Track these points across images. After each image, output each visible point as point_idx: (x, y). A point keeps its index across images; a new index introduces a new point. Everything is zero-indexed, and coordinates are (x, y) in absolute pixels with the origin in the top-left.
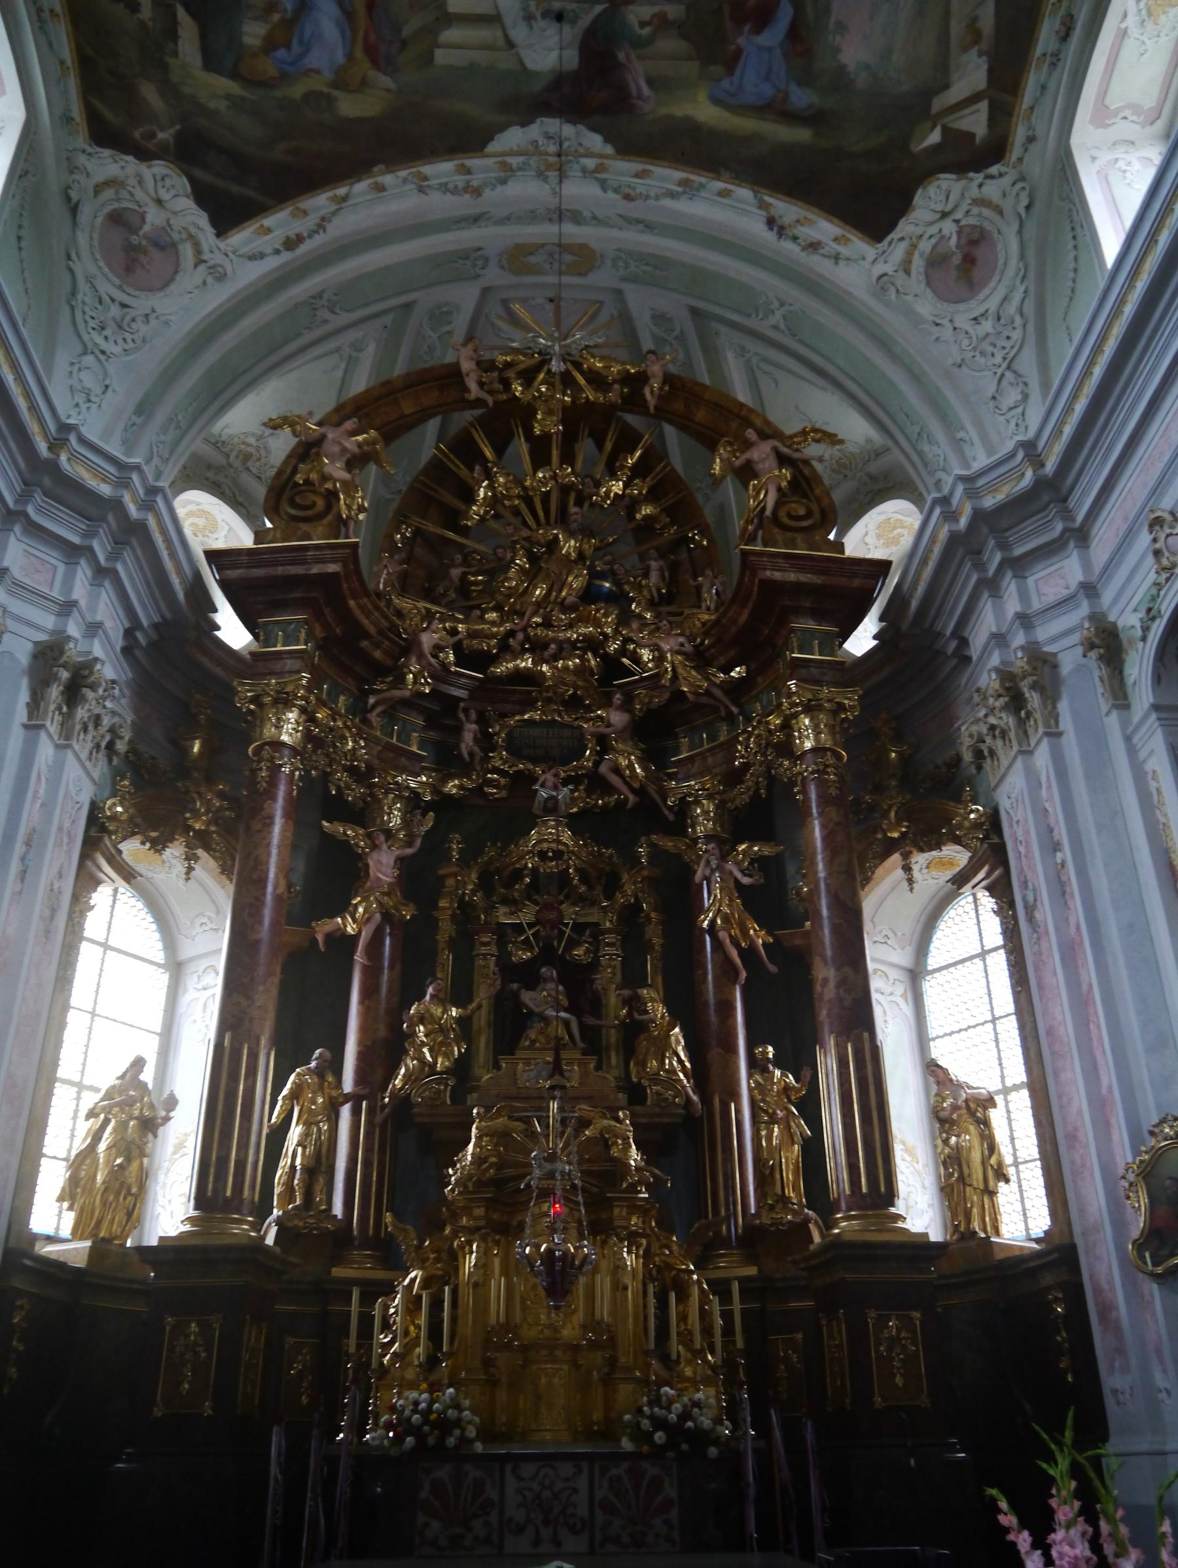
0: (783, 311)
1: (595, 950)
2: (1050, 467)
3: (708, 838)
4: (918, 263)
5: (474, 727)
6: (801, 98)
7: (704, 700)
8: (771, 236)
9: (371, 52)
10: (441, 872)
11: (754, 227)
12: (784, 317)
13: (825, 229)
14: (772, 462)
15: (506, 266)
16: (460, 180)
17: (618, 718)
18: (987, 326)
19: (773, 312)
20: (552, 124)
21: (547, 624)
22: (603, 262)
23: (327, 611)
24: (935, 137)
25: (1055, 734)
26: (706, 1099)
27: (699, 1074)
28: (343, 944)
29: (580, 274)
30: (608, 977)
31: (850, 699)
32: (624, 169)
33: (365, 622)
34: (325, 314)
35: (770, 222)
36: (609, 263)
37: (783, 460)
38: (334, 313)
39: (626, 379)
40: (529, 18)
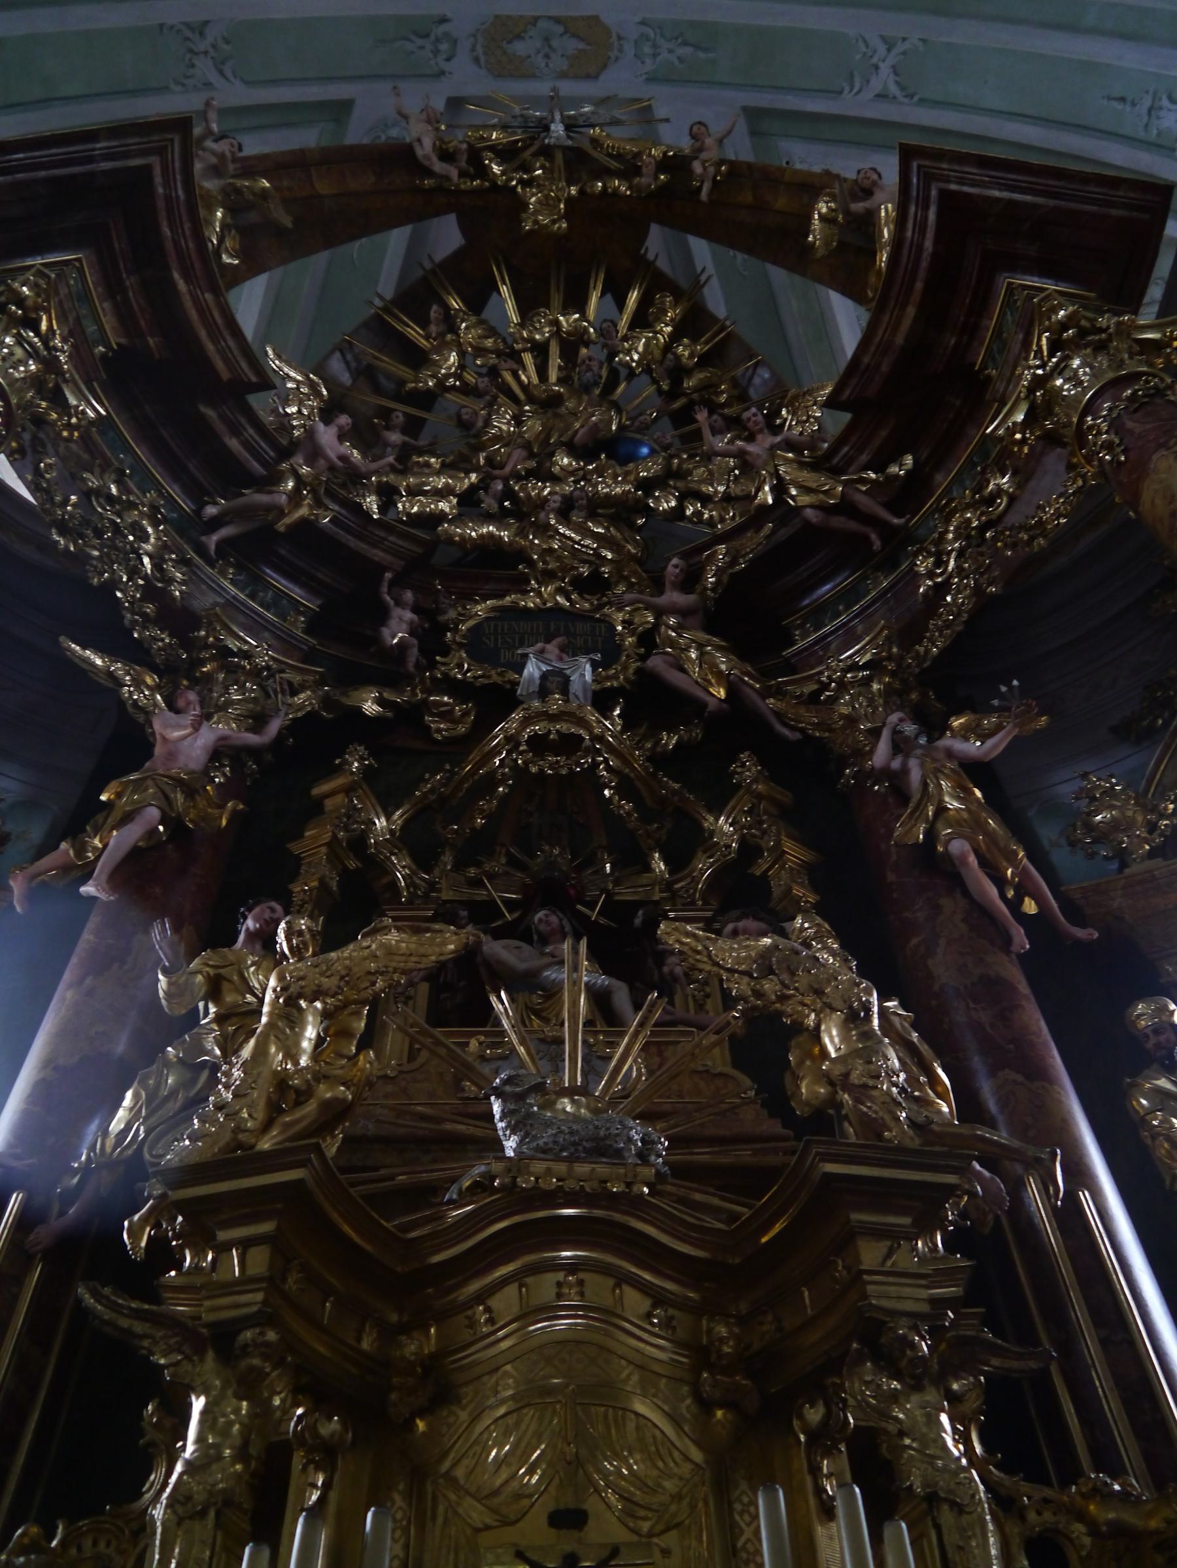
0: (891, 60)
5: (408, 615)
7: (838, 522)
10: (316, 791)
12: (895, 70)
15: (482, 60)
19: (877, 68)
22: (621, 50)
23: (130, 282)
29: (588, 77)
33: (210, 347)
34: (205, 68)
36: (629, 49)
38: (221, 73)
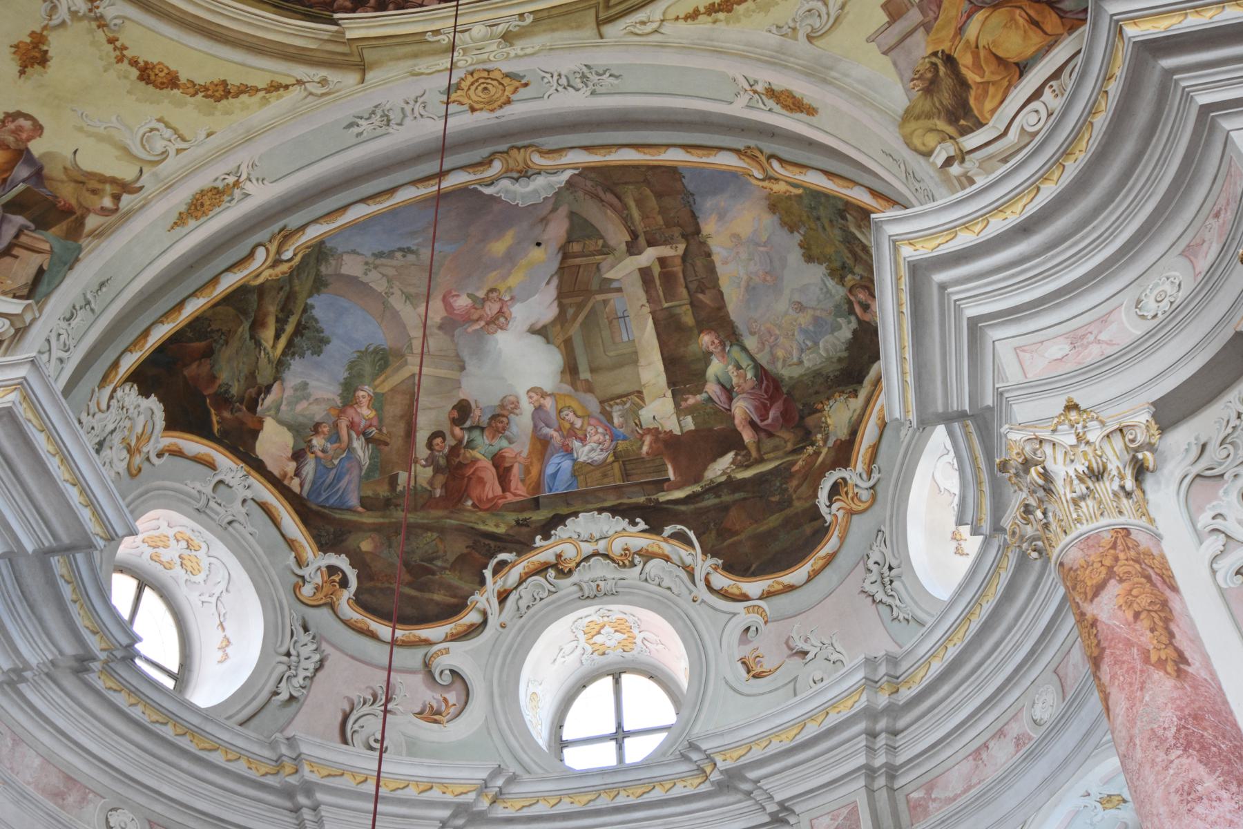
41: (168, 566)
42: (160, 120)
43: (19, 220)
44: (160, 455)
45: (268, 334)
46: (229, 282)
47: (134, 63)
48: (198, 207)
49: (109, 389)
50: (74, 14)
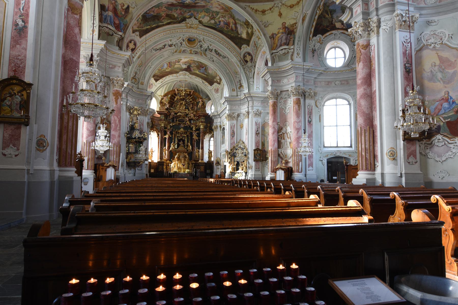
1: (185, 138)
2: (219, 114)
3: (194, 130)
4: (214, 89)
6: (206, 73)
8: (202, 83)
9: (169, 67)
11: (202, 82)
13: (207, 84)
14: (201, 101)
16: (176, 76)
17: (188, 119)
18: (218, 96)
20: (185, 72)
21: (182, 111)
24: (216, 80)
25: (217, 131)
26: (192, 151)
27: (192, 149)
28: (166, 138)
30: (186, 141)
31: (205, 124)
32: (190, 75)
35: (202, 82)
37: (202, 101)
39: (189, 91)
40: (183, 64)
41: (337, 45)
42: (295, 12)
43: (289, 36)
44: (324, 38)
45: (327, 16)
46: (316, 18)
47: (289, 6)
48: (303, 20)
49: (311, 41)
50: (281, 6)
